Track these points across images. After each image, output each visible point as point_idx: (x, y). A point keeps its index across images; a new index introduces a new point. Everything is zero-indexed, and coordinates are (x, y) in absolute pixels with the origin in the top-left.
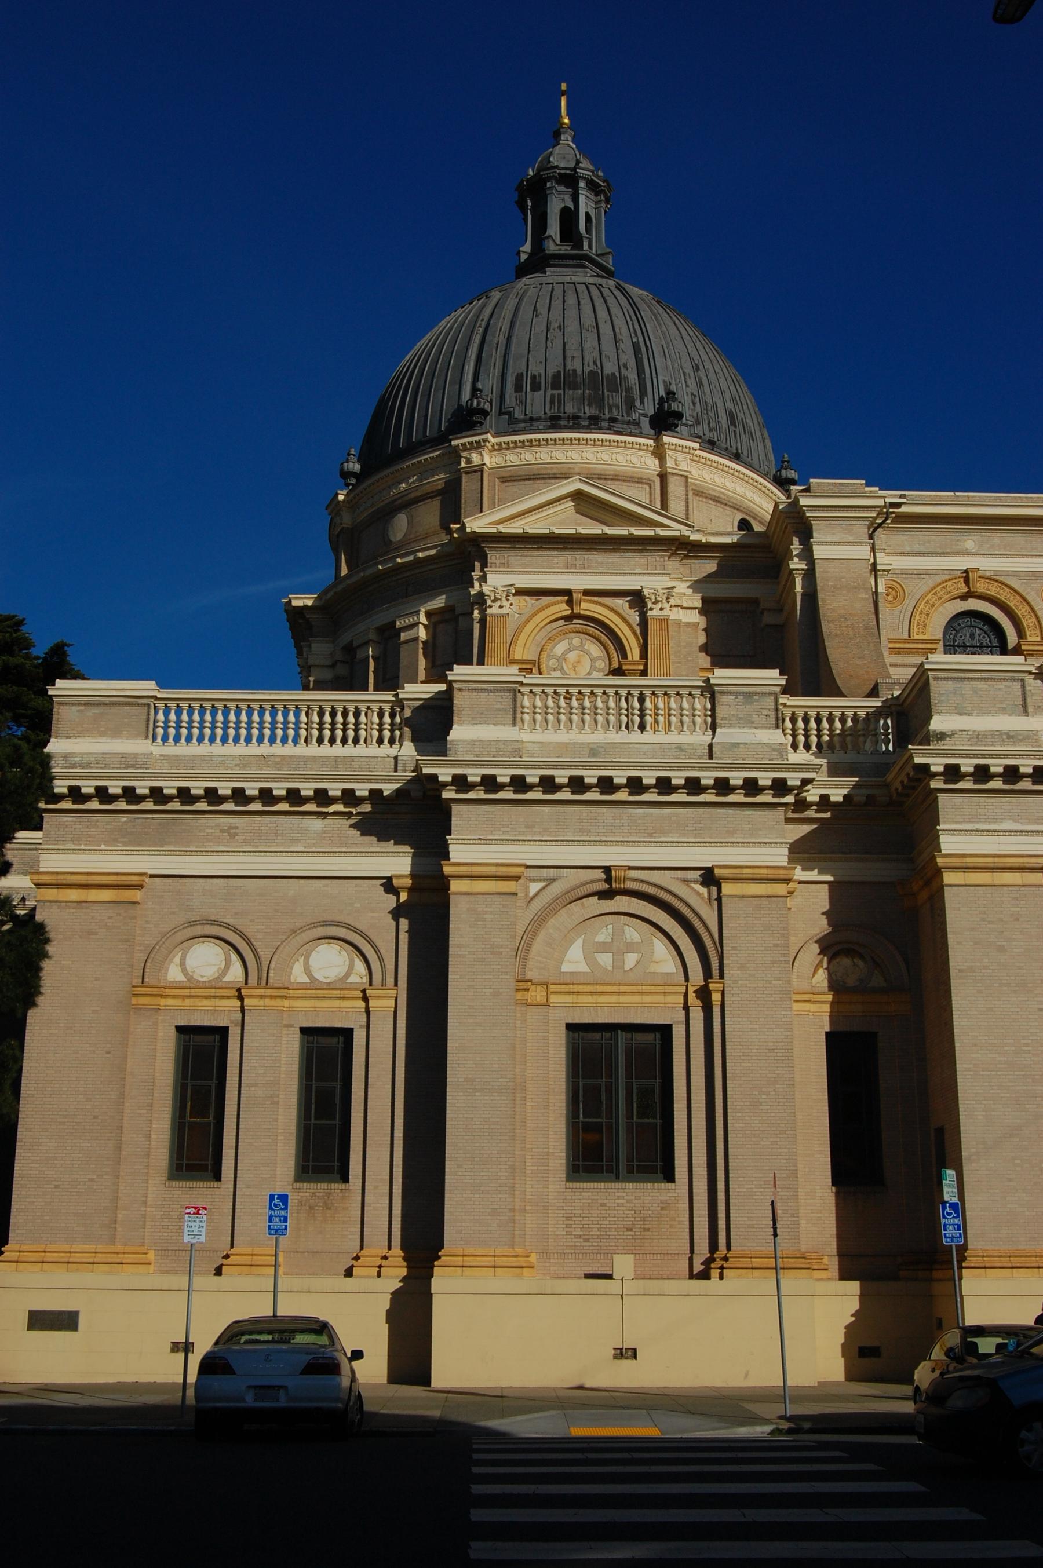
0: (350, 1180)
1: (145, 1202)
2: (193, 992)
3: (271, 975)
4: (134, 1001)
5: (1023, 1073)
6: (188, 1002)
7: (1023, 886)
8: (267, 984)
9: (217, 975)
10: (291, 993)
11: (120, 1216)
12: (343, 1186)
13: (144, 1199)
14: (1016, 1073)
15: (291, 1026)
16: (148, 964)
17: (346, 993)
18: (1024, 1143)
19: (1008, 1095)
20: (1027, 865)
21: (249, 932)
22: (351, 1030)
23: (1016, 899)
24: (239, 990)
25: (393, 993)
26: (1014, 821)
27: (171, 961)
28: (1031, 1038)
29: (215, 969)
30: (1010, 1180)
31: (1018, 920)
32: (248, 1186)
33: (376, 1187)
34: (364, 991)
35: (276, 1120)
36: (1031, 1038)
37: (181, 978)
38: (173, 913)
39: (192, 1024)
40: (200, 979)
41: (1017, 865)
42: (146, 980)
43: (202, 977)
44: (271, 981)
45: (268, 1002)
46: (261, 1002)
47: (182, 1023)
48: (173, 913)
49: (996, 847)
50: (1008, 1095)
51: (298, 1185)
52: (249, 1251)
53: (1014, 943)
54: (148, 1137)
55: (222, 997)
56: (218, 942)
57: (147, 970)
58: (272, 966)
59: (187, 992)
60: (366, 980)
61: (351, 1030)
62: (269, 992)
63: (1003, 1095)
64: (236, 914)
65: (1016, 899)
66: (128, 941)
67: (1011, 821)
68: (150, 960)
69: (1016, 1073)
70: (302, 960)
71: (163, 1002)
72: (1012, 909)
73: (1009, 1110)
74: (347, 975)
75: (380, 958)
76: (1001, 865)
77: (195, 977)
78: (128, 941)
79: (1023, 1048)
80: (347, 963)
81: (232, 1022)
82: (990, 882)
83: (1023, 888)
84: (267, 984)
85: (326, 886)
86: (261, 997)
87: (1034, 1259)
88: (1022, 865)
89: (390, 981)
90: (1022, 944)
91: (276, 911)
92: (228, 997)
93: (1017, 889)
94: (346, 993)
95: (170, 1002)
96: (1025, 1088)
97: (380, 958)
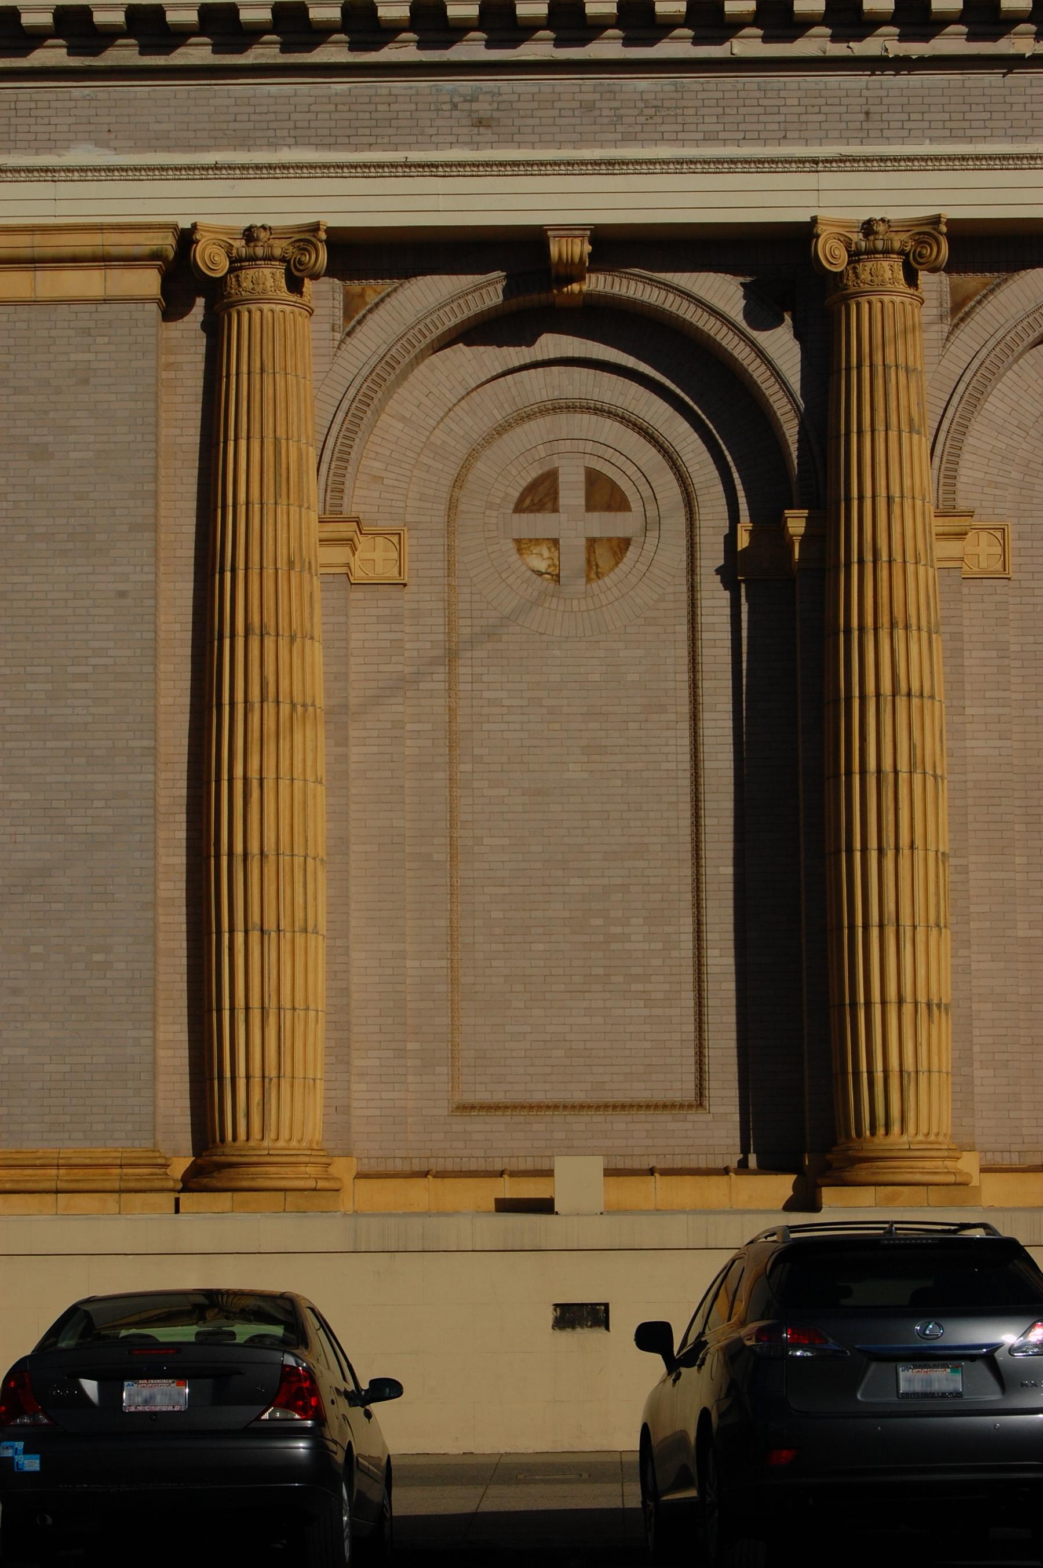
5: (68, 744)
7: (105, 301)
14: (49, 744)
18: (54, 906)
19: (26, 796)
20: (114, 251)
23: (87, 332)
26: (101, 144)
28: (93, 661)
30: (15, 992)
31: (86, 381)
36: (93, 661)
41: (88, 251)
49: (48, 208)
50: (26, 796)
53: (72, 438)
63: (12, 796)
65: (87, 332)
67: (90, 147)
69: (49, 744)
72: (73, 357)
73: (27, 830)
76: (50, 252)
79: (71, 686)
82: (25, 293)
83: (106, 307)
87: (54, 1172)
88: (99, 251)
90: (92, 438)
93: (92, 308)
96: (68, 778)
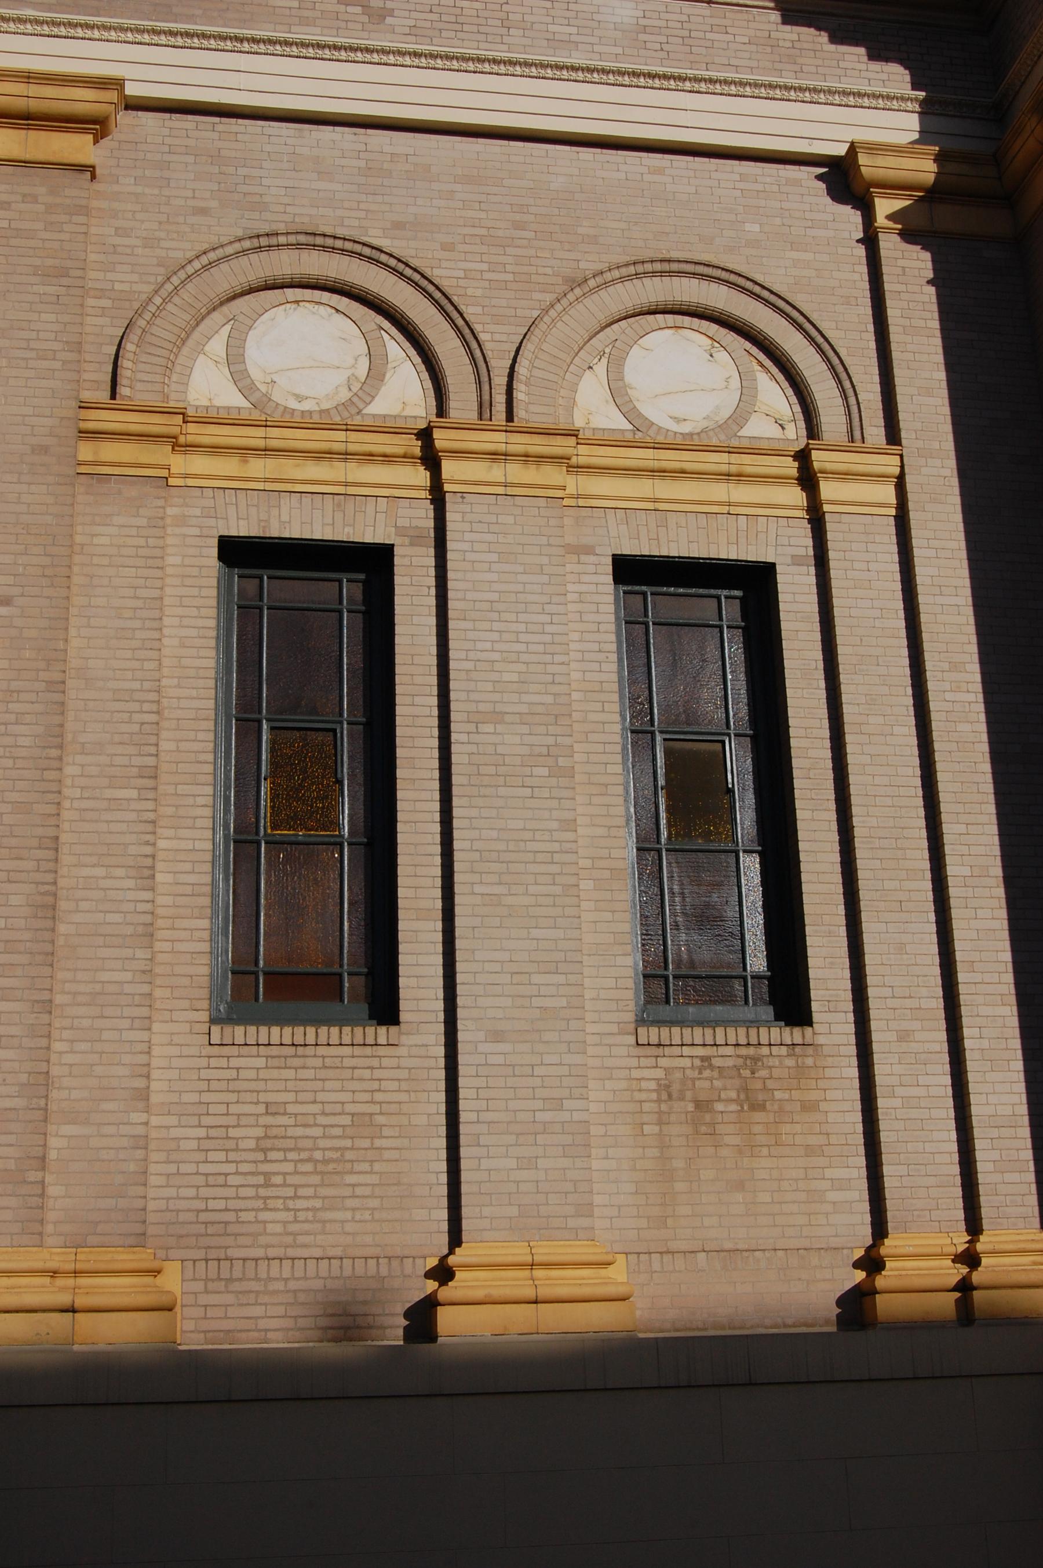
0: (816, 1017)
1: (143, 1095)
2: (277, 437)
3: (519, 395)
4: (86, 451)
6: (258, 467)
8: (510, 417)
9: (344, 395)
10: (584, 455)
11: (53, 1142)
12: (796, 1034)
13: (140, 1083)
15: (589, 550)
16: (129, 346)
17: (749, 464)
21: (444, 275)
22: (769, 569)
24: (425, 435)
25: (890, 465)
27: (200, 349)
29: (341, 377)
32: (497, 1036)
33: (904, 1036)
34: (803, 457)
35: (570, 825)
37: (231, 398)
38: (203, 211)
39: (275, 531)
40: (293, 404)
42: (123, 391)
43: (300, 398)
44: (520, 412)
45: (516, 472)
46: (496, 472)
47: (242, 528)
48: (203, 211)
51: (653, 1034)
52: (519, 1252)
54: (147, 877)
55: (369, 457)
56: (344, 302)
57: (125, 363)
58: (521, 370)
59: (254, 437)
60: (795, 434)
61: (769, 569)
62: (519, 443)
64: (398, 226)
66: (64, 273)
68: (133, 337)
70: (601, 368)
71: (179, 463)
74: (740, 416)
75: (839, 372)
77: (277, 396)
78: (64, 273)
80: (735, 382)
81: (400, 531)
84: (510, 417)
85: (660, 171)
86: (495, 456)
89: (876, 433)
91: (518, 226)
92: (387, 459)
94: (749, 464)
95: (199, 464)
97: (839, 372)
